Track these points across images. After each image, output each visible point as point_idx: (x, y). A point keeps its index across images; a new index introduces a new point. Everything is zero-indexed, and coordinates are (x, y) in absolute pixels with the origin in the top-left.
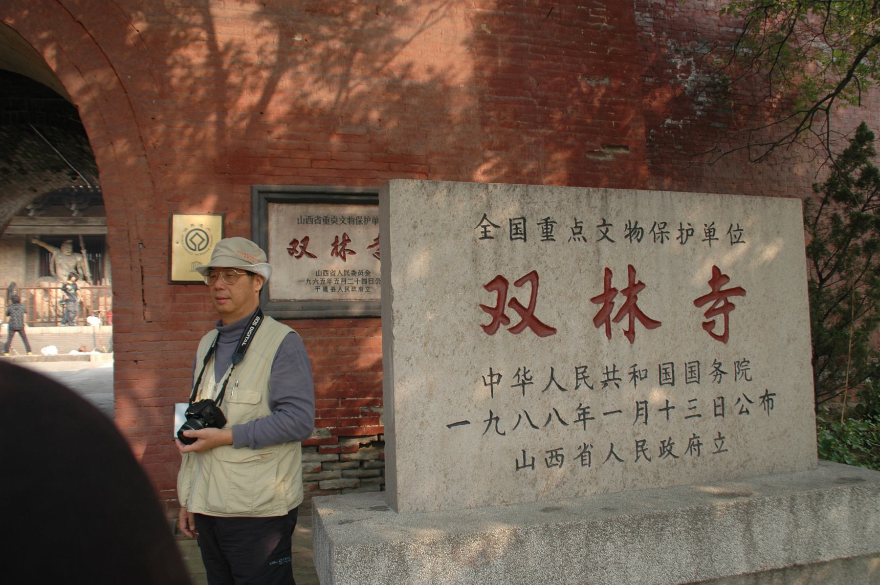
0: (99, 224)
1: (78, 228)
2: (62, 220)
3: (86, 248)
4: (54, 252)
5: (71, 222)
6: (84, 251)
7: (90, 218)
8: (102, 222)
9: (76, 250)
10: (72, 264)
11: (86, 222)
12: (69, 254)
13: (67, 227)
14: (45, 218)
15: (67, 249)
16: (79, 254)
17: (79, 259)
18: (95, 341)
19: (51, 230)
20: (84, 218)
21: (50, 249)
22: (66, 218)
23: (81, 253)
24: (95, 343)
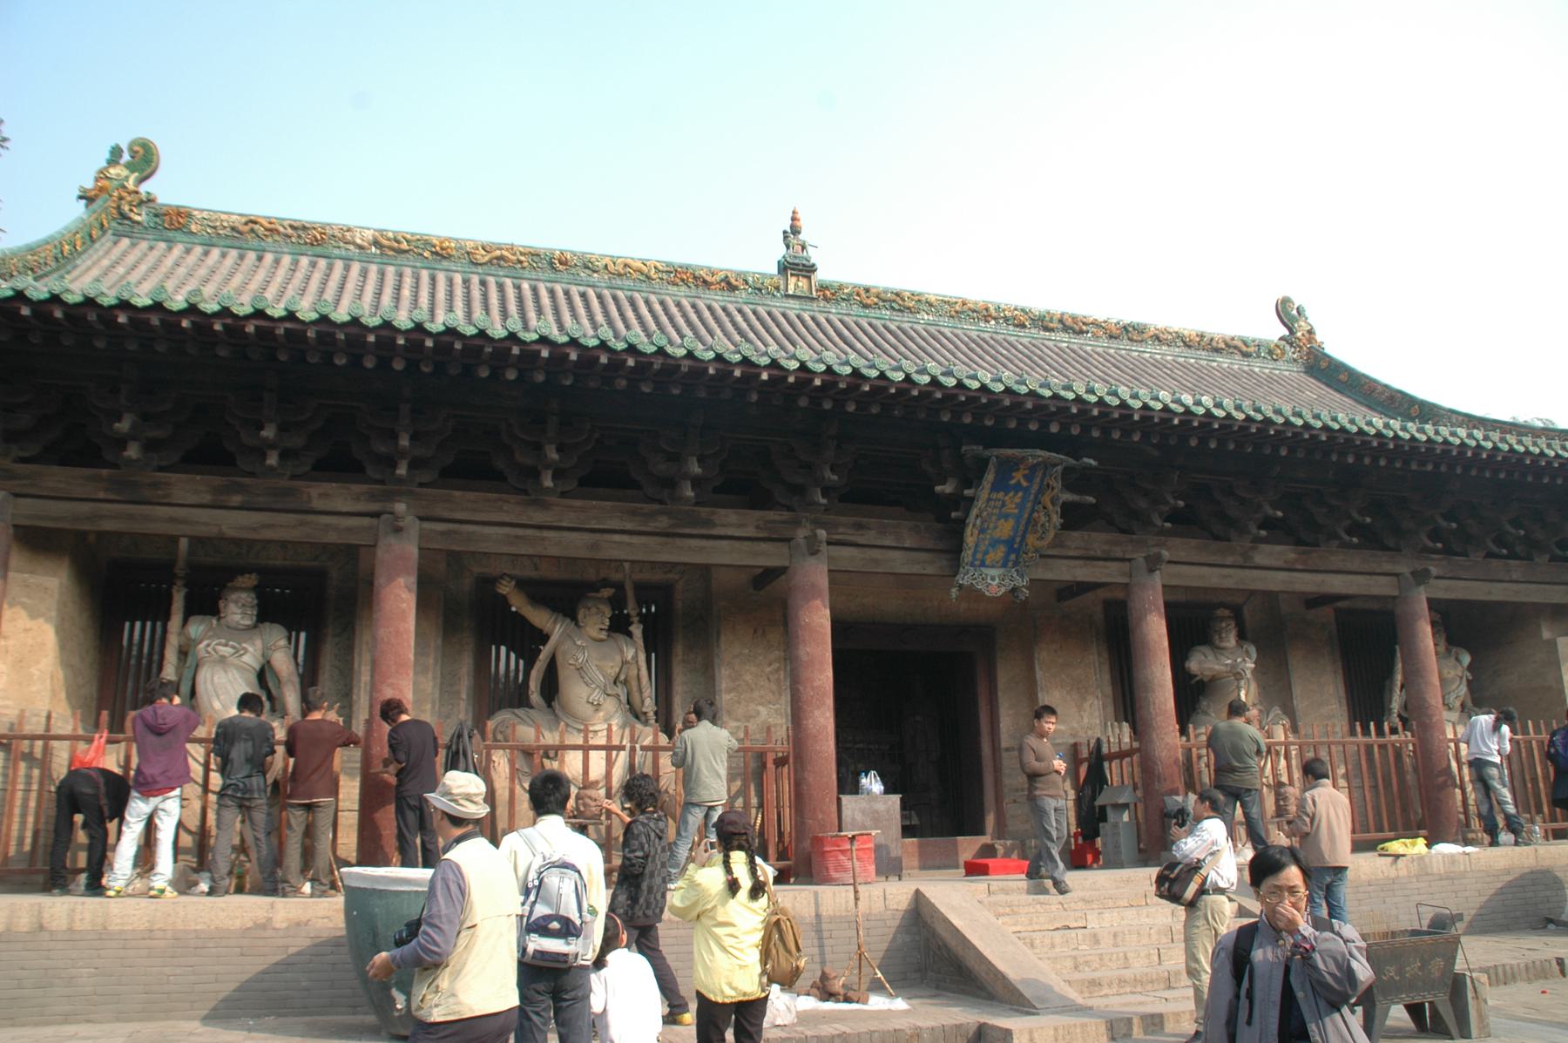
0: (750, 532)
1: (678, 541)
2: (633, 513)
3: (644, 619)
4: (557, 629)
5: (663, 523)
6: (637, 630)
7: (722, 511)
8: (758, 527)
9: (619, 626)
10: (612, 668)
11: (709, 523)
12: (603, 635)
13: (643, 539)
14: (578, 503)
15: (595, 622)
16: (628, 639)
17: (629, 653)
18: (821, 946)
19: (595, 546)
20: (704, 511)
21: (539, 618)
22: (647, 507)
23: (630, 635)
24: (822, 954)
